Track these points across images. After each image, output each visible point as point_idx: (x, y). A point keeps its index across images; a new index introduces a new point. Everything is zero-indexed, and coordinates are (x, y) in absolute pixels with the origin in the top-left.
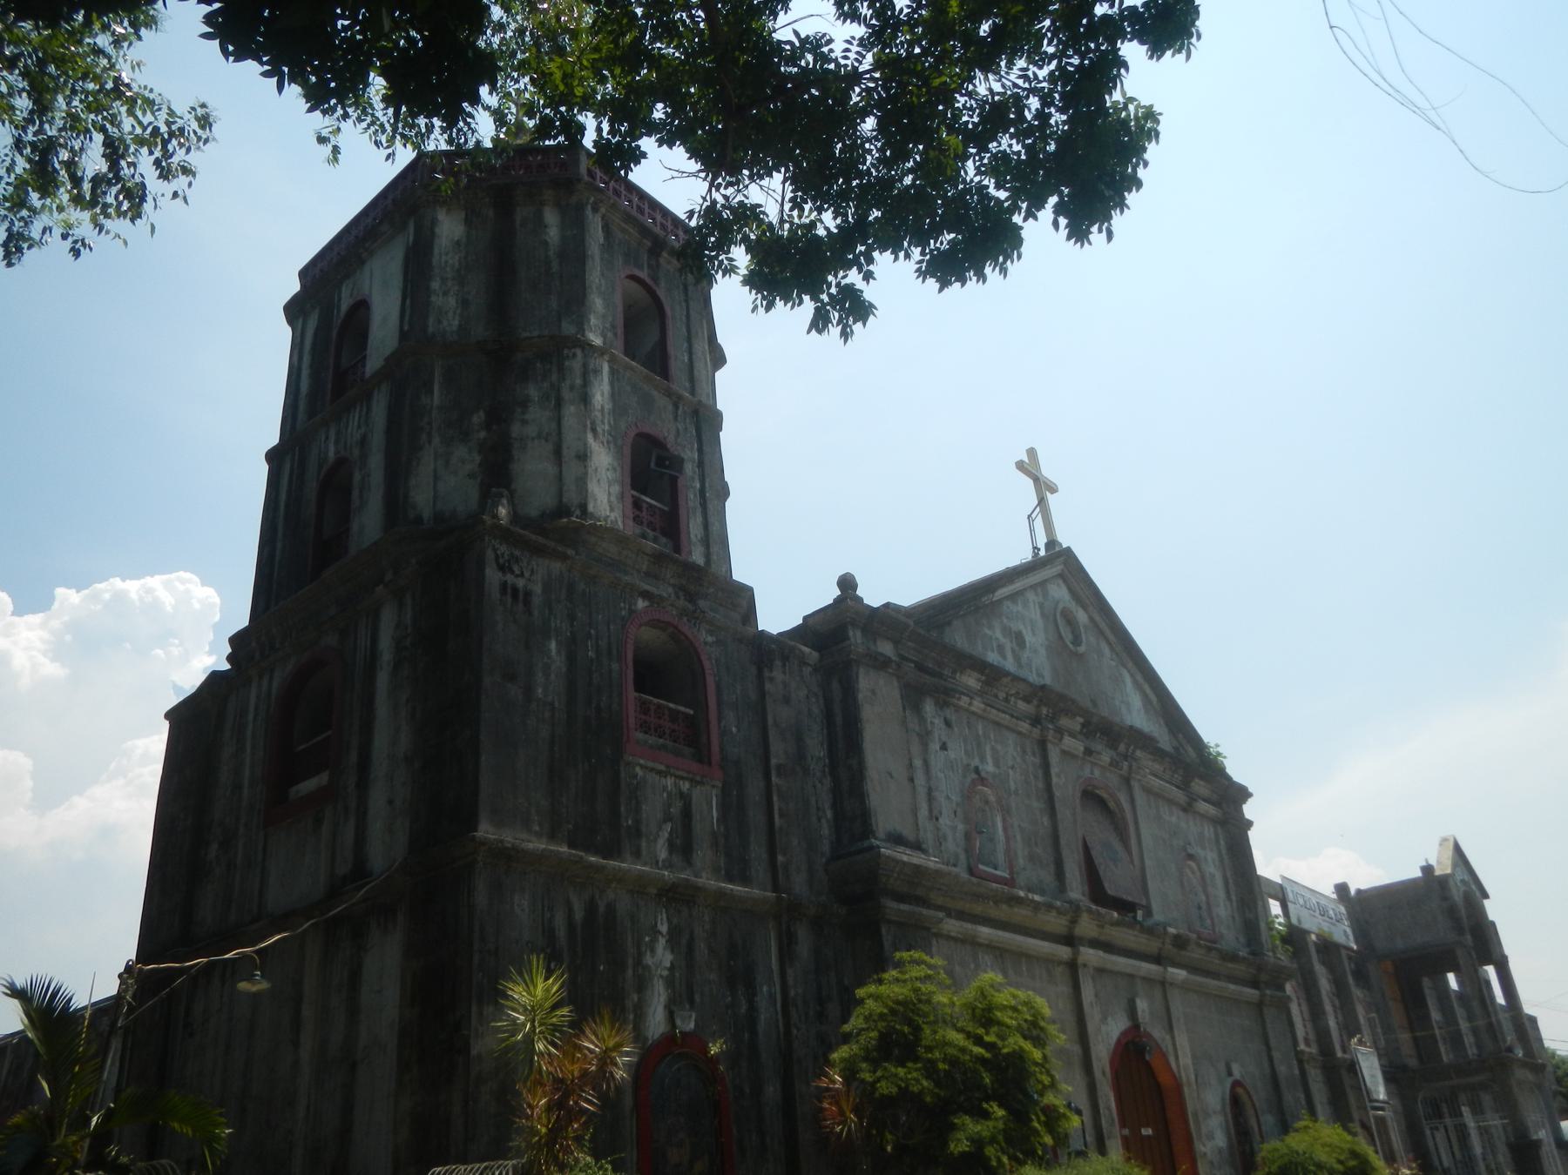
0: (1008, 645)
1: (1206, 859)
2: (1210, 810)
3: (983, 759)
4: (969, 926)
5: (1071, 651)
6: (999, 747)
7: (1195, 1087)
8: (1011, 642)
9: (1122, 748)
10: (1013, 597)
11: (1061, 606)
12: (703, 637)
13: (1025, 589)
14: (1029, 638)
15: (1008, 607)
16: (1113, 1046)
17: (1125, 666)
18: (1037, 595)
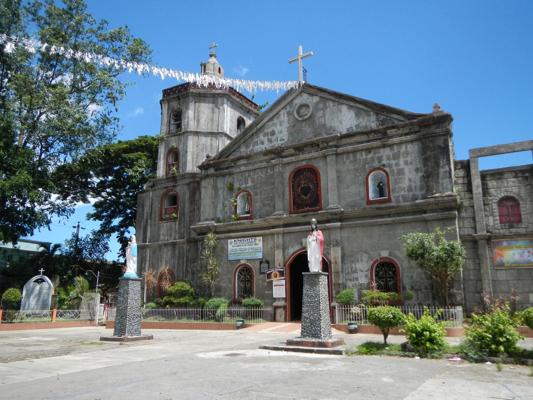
0: (265, 140)
1: (397, 164)
2: (404, 138)
3: (247, 183)
4: (227, 234)
5: (302, 121)
6: (255, 176)
7: (340, 264)
8: (268, 136)
9: (321, 146)
10: (271, 119)
11: (297, 107)
12: (178, 189)
13: (280, 111)
14: (277, 129)
15: (268, 125)
16: (290, 255)
17: (344, 104)
18: (286, 109)
